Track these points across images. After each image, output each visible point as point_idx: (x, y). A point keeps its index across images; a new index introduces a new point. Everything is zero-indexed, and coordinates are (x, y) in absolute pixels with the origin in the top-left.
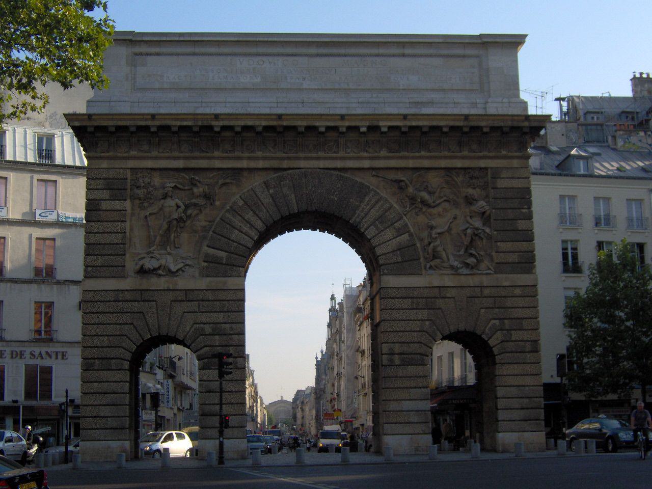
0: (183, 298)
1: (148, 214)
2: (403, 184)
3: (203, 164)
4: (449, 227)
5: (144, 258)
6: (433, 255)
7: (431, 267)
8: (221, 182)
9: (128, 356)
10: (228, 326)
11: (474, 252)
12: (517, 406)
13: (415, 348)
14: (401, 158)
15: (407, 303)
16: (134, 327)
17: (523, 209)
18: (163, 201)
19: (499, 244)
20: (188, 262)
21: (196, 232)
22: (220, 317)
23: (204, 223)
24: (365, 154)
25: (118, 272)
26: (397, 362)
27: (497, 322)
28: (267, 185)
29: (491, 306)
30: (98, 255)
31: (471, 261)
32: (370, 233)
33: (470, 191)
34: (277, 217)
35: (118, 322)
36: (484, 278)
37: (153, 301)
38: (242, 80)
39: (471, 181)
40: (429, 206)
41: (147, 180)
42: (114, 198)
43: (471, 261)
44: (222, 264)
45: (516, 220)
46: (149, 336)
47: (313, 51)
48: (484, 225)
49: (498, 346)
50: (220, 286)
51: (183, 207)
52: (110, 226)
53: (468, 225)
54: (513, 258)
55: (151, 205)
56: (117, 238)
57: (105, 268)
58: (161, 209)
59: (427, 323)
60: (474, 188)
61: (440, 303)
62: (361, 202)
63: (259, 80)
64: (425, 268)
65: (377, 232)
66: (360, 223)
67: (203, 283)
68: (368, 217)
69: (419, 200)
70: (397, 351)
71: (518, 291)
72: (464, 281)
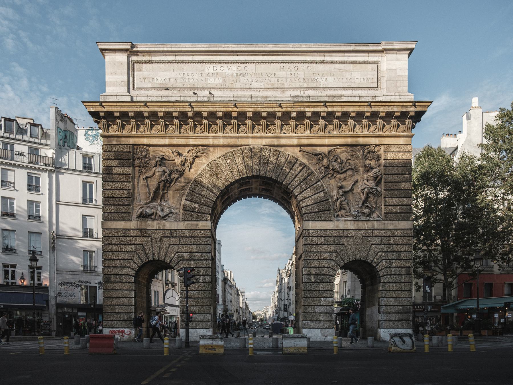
0: (169, 235)
1: (145, 177)
2: (320, 156)
3: (182, 141)
4: (352, 187)
5: (142, 207)
6: (340, 207)
7: (338, 216)
8: (194, 154)
9: (133, 273)
10: (199, 254)
11: (369, 205)
12: (394, 311)
13: (325, 271)
14: (320, 137)
15: (321, 240)
16: (137, 254)
17: (405, 174)
18: (154, 168)
19: (387, 199)
20: (174, 211)
21: (178, 190)
22: (194, 248)
23: (183, 184)
24: (294, 135)
25: (126, 216)
26: (313, 280)
27: (383, 254)
28: (225, 156)
29: (379, 243)
30: (111, 205)
31: (366, 211)
32: (296, 191)
33: (368, 162)
34: (233, 180)
35: (126, 250)
36: (375, 223)
37: (149, 237)
38: (209, 82)
39: (369, 155)
40: (338, 172)
41: (143, 154)
42: (121, 166)
43: (366, 211)
44: (195, 212)
45: (400, 182)
46: (147, 260)
47: (259, 58)
48: (376, 186)
49: (383, 270)
50: (194, 227)
51: (168, 172)
52: (119, 185)
53: (365, 186)
54: (397, 209)
55: (147, 171)
56: (124, 194)
57: (116, 214)
58: (154, 174)
59: (334, 254)
60: (371, 160)
61: (344, 240)
62: (291, 169)
63: (221, 81)
64: (334, 217)
65: (301, 191)
66: (290, 184)
67: (182, 225)
68: (295, 180)
69: (332, 168)
70: (313, 273)
71: (398, 233)
72: (361, 225)
